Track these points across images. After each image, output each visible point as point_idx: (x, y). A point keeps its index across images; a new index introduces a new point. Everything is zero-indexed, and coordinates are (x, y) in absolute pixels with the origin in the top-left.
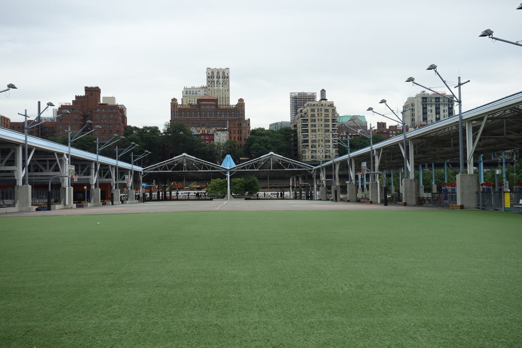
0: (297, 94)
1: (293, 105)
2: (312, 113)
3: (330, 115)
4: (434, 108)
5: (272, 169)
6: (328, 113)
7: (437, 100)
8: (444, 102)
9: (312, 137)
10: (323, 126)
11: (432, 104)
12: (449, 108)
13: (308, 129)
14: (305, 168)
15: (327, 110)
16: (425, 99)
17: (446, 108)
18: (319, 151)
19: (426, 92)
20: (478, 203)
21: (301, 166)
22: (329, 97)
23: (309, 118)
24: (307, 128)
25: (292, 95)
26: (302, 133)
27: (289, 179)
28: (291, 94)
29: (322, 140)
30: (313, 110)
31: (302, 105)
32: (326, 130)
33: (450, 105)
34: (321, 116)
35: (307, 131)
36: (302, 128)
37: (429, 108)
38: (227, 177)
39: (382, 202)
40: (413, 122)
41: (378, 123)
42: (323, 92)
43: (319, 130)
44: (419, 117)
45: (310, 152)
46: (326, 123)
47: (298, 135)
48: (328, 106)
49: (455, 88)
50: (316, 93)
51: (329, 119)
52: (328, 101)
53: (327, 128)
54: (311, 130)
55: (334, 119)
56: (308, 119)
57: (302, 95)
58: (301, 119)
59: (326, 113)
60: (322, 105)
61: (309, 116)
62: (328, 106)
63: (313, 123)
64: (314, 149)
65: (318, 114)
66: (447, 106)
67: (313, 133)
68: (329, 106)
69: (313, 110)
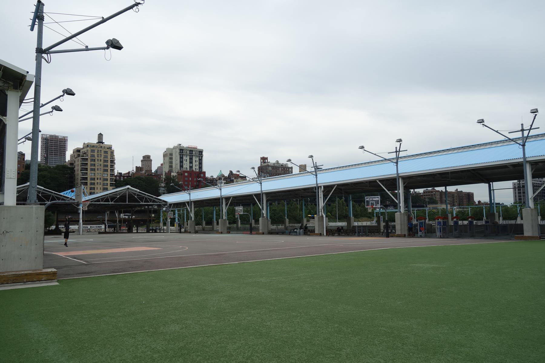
0: (48, 136)
1: (43, 145)
2: (92, 153)
3: (109, 157)
4: (188, 158)
5: (127, 203)
6: (107, 155)
7: (191, 152)
8: (196, 154)
9: (91, 175)
10: (102, 165)
11: (187, 155)
12: (199, 159)
13: (87, 168)
14: (160, 202)
15: (106, 152)
16: (182, 151)
17: (197, 159)
18: (97, 188)
19: (181, 145)
20: (399, 236)
21: (156, 200)
22: (107, 141)
23: (89, 158)
24: (86, 166)
25: (44, 136)
26: (81, 171)
27: (104, 212)
28: (43, 136)
29: (100, 179)
30: (93, 151)
31: (53, 146)
32: (105, 169)
33: (200, 157)
34: (101, 157)
35: (86, 169)
36: (81, 166)
37: (184, 158)
38: (80, 210)
39: (327, 234)
40: (170, 168)
41: (136, 167)
42: (100, 136)
43: (98, 169)
44: (176, 164)
45: (89, 189)
46: (105, 164)
47: (76, 173)
48: (107, 148)
49: (509, 133)
50: (67, 137)
51: (108, 160)
52: (105, 144)
53: (106, 168)
54: (90, 169)
55: (112, 161)
56: (87, 159)
57: (54, 138)
58: (81, 158)
59: (105, 155)
60: (101, 147)
61: (89, 156)
62: (107, 148)
63: (93, 163)
64: (92, 186)
65: (98, 155)
66: (198, 158)
67: (93, 172)
68: (108, 149)
69: (93, 151)
